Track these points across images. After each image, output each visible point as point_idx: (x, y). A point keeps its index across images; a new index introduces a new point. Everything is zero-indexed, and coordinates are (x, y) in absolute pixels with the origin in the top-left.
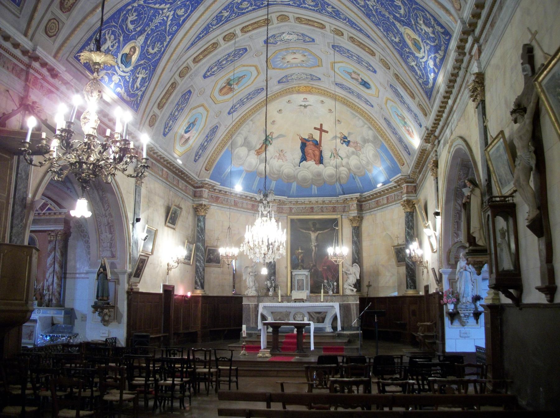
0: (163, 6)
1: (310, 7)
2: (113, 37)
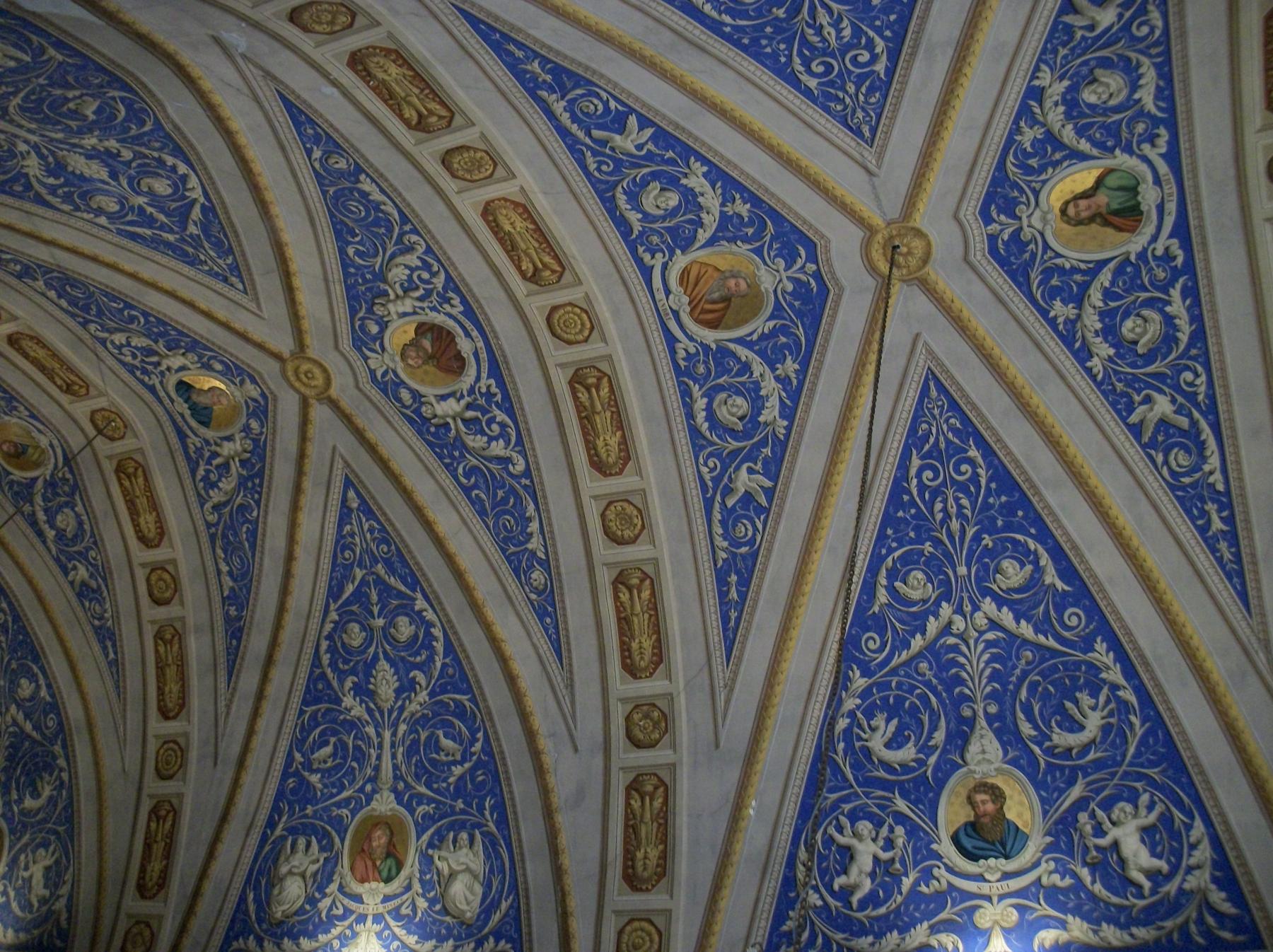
2: (865, 827)
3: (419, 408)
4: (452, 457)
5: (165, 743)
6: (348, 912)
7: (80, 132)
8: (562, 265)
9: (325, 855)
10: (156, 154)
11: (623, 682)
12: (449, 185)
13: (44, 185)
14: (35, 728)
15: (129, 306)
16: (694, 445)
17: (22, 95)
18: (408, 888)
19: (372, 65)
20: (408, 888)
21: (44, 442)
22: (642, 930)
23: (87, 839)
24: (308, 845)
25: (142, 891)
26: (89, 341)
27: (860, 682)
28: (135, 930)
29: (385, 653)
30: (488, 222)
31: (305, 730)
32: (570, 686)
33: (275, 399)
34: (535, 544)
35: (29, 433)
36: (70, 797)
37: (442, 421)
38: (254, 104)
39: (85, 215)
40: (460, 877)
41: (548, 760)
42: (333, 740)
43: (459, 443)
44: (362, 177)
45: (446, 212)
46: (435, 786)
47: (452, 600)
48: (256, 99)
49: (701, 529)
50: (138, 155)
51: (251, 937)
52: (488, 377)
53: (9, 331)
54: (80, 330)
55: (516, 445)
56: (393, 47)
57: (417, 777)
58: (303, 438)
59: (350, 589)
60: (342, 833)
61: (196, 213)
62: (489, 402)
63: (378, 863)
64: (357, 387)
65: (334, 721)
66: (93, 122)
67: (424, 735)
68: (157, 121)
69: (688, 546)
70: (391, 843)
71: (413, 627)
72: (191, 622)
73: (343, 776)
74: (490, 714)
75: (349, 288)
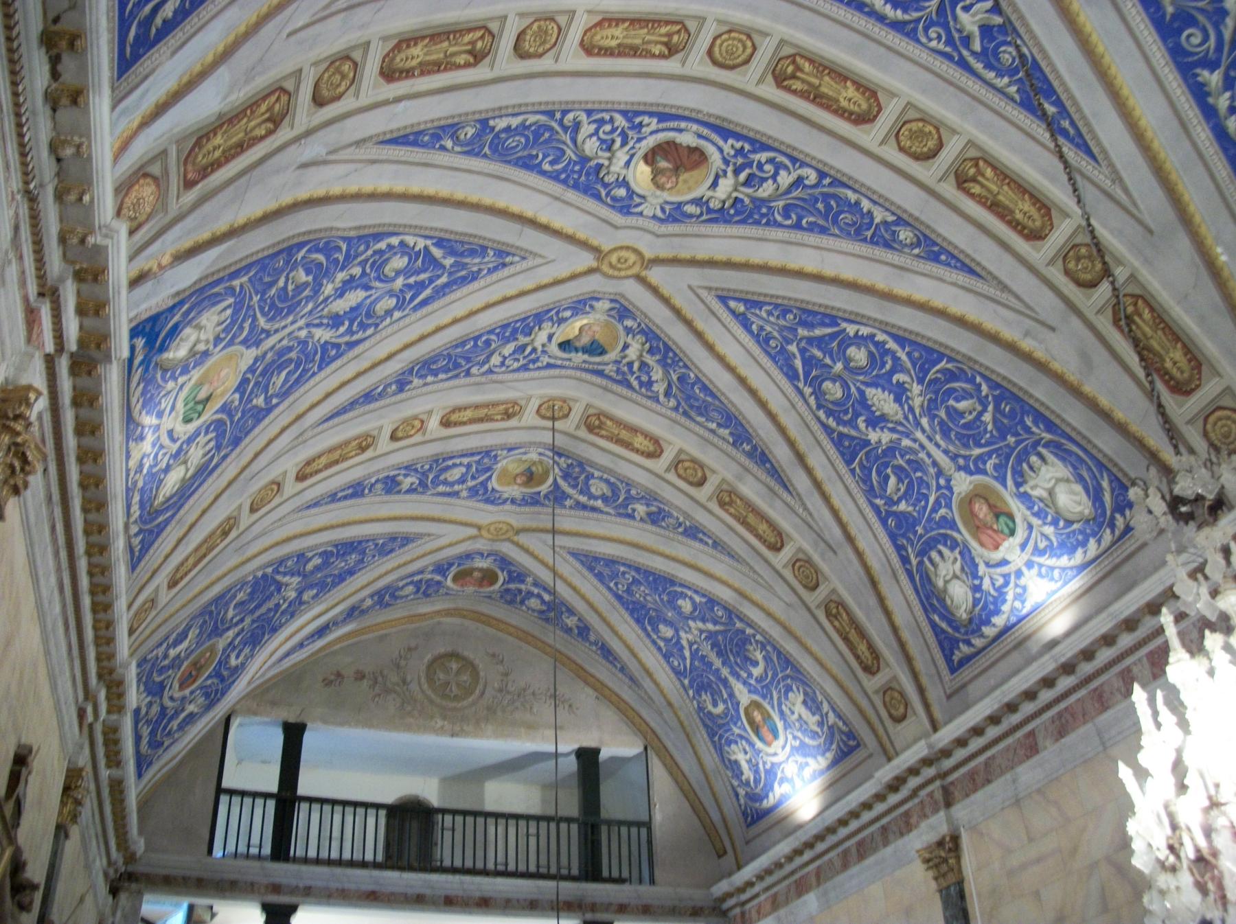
0: (684, 643)
1: (457, 461)
3: (708, 207)
4: (763, 215)
5: (793, 565)
6: (1006, 577)
7: (316, 292)
8: (679, 23)
9: (957, 551)
10: (370, 252)
11: (1039, 251)
12: (546, 63)
13: (342, 335)
14: (715, 623)
15: (476, 339)
16: (907, 35)
17: (259, 315)
18: (1030, 527)
19: (401, 65)
20: (1030, 527)
21: (533, 456)
22: (1220, 419)
23: (807, 664)
24: (940, 553)
25: (867, 669)
26: (483, 379)
27: (1214, 79)
28: (887, 699)
29: (863, 383)
30: (598, 54)
31: (866, 479)
32: (1005, 288)
33: (623, 296)
34: (879, 215)
35: (520, 460)
36: (775, 648)
37: (731, 201)
38: (376, 166)
39: (384, 323)
40: (1057, 490)
41: (1040, 354)
42: (889, 471)
43: (758, 202)
44: (491, 123)
45: (568, 80)
46: (983, 441)
47: (868, 306)
48: (374, 162)
49: (977, 87)
50: (363, 264)
51: (961, 645)
52: (726, 141)
53: (437, 422)
54: (468, 380)
55: (794, 165)
56: (395, 41)
57: (966, 446)
58: (666, 301)
59: (798, 363)
60: (953, 526)
61: (437, 253)
62: (745, 156)
63: (995, 527)
64: (658, 236)
65: (877, 458)
66: (315, 279)
67: (942, 414)
68: (344, 239)
69: (981, 108)
70: (991, 507)
71: (863, 349)
72: (729, 477)
73: (919, 489)
74: (970, 359)
75: (576, 187)
